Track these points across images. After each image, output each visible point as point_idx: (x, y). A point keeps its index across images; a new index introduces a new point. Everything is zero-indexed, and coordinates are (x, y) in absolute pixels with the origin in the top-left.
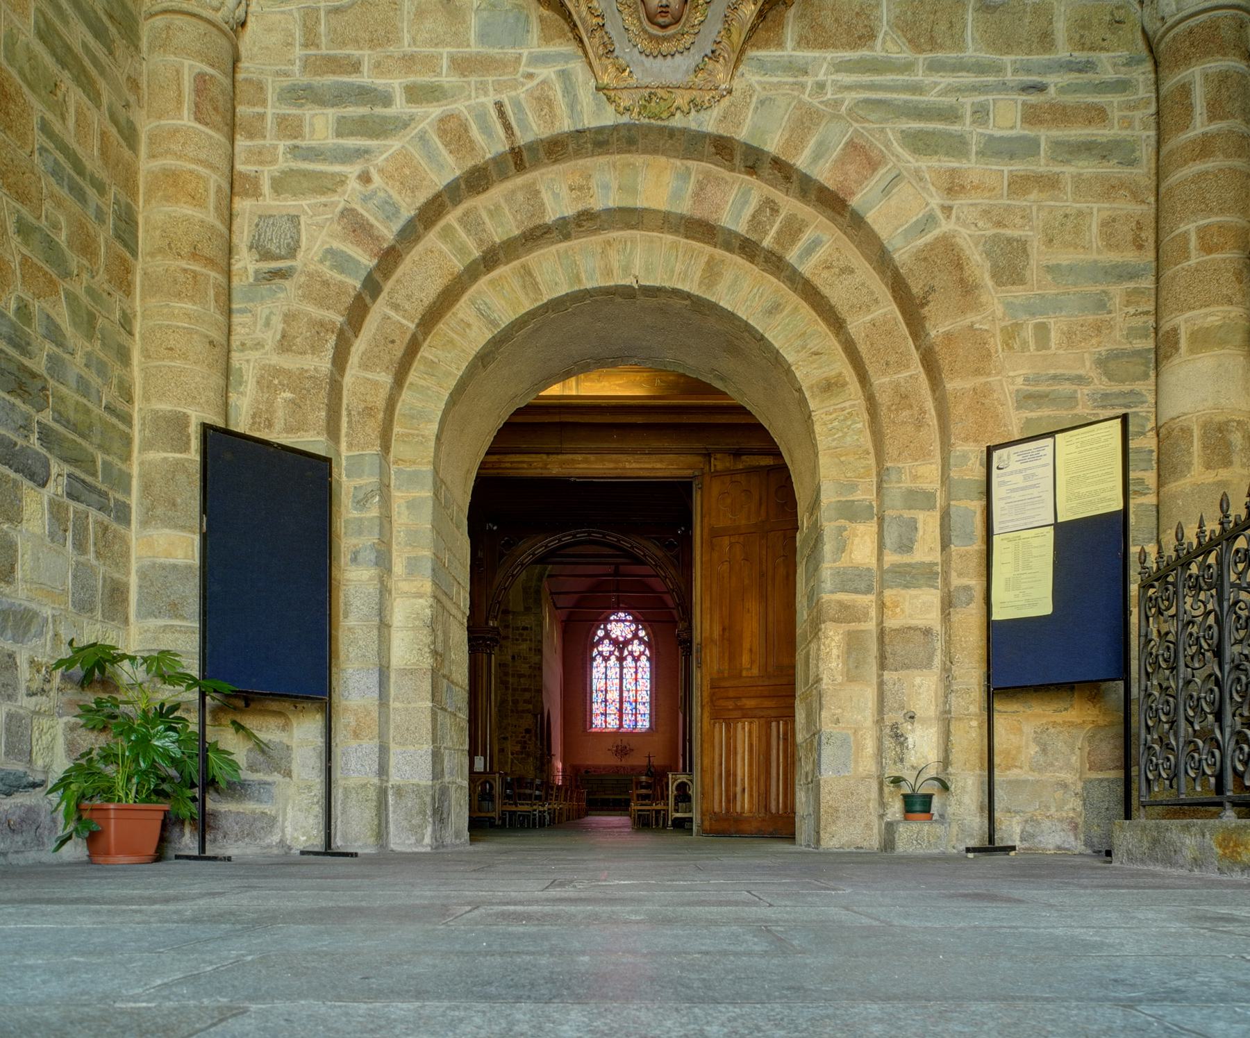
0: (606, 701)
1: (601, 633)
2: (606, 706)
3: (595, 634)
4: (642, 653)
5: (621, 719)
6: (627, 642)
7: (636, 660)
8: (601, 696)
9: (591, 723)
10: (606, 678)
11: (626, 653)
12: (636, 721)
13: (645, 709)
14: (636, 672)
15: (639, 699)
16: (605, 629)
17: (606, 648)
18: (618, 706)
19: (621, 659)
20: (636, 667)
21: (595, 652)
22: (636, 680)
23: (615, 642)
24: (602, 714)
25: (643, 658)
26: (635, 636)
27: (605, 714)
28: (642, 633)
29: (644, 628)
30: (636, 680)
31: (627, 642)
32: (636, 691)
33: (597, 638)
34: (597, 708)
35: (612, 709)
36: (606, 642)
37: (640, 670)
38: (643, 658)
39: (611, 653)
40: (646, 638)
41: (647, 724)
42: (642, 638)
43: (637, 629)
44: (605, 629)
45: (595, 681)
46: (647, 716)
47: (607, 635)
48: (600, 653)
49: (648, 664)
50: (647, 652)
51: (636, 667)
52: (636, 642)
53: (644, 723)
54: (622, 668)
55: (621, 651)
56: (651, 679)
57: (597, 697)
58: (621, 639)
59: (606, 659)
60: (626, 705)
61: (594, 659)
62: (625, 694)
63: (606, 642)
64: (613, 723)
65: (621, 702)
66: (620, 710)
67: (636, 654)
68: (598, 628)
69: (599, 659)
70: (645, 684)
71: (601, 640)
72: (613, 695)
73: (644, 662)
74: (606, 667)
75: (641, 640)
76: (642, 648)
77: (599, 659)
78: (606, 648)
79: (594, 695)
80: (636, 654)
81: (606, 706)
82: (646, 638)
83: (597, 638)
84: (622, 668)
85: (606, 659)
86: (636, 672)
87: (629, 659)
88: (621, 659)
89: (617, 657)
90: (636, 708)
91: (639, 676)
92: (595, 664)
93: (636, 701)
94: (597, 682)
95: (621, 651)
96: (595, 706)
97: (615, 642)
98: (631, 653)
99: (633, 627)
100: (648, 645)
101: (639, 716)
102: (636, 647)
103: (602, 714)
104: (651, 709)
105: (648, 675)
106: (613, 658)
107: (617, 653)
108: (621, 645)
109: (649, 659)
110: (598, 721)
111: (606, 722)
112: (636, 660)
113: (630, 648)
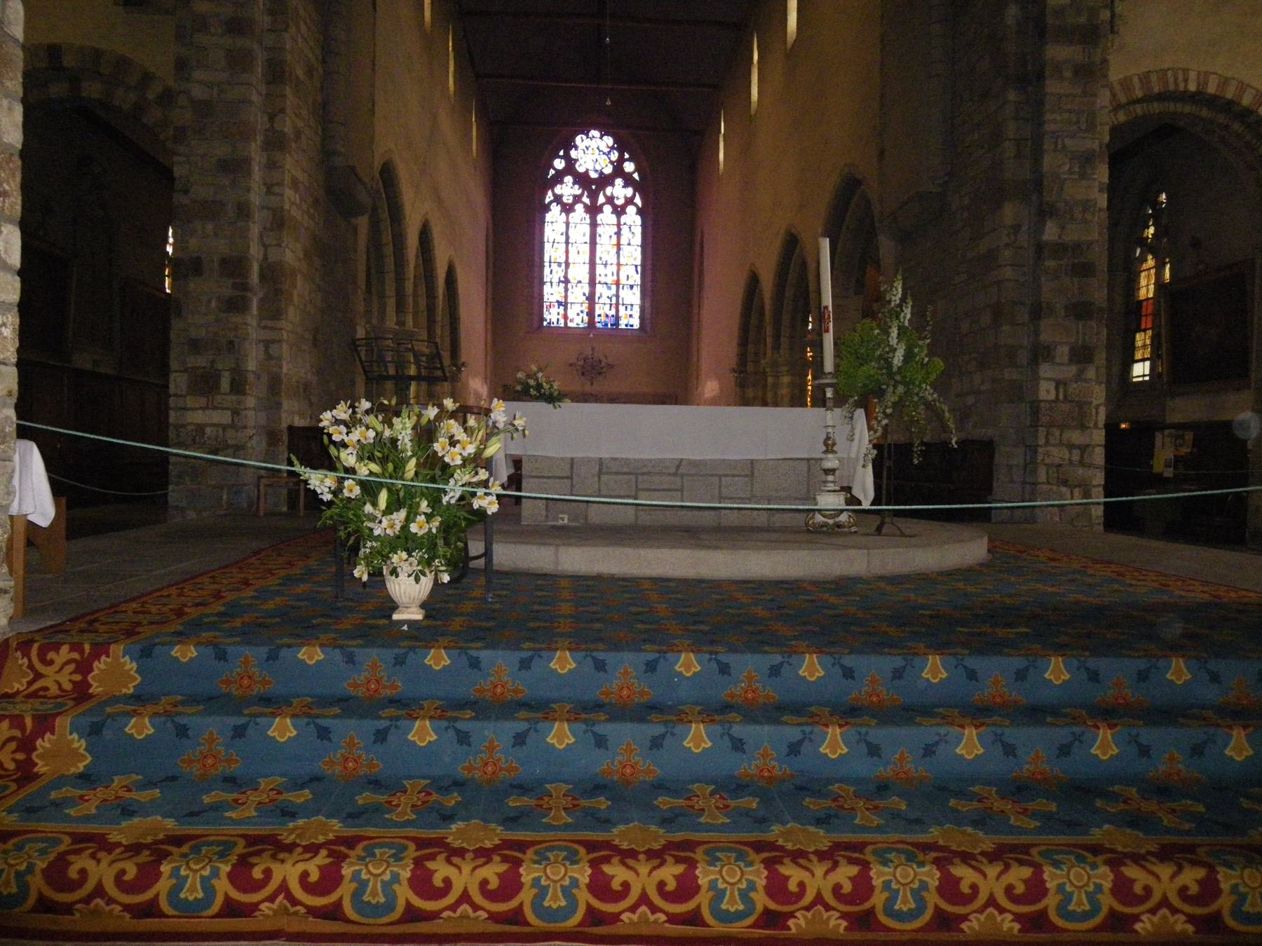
1: (559, 164)
2: (566, 290)
4: (629, 201)
5: (591, 313)
6: (605, 181)
7: (619, 211)
8: (559, 273)
9: (543, 319)
10: (567, 243)
11: (601, 199)
13: (633, 297)
14: (618, 234)
15: (623, 280)
16: (567, 157)
17: (568, 189)
18: (587, 290)
19: (594, 210)
20: (619, 225)
21: (549, 197)
22: (618, 245)
23: (582, 180)
25: (631, 210)
26: (618, 171)
27: (564, 304)
28: (629, 167)
30: (618, 245)
31: (605, 181)
32: (619, 265)
33: (552, 172)
34: (551, 293)
35: (578, 295)
36: (569, 179)
37: (625, 230)
39: (577, 199)
40: (636, 176)
41: (636, 323)
42: (630, 174)
43: (621, 160)
44: (567, 157)
45: (547, 247)
47: (571, 163)
48: (558, 199)
49: (638, 220)
50: (638, 200)
51: (619, 225)
53: (631, 319)
54: (594, 225)
55: (593, 196)
56: (644, 246)
57: (551, 274)
58: (594, 175)
59: (567, 209)
60: (599, 289)
61: (547, 208)
62: (600, 269)
63: (569, 179)
64: (577, 319)
65: (593, 283)
66: (591, 299)
67: (620, 202)
69: (555, 208)
70: (633, 254)
72: (579, 272)
73: (632, 217)
74: (567, 224)
75: (628, 181)
77: (555, 208)
78: (568, 189)
79: (547, 270)
81: (566, 290)
82: (636, 176)
83: (552, 172)
84: (594, 225)
85: (567, 209)
86: (618, 234)
87: (608, 209)
88: (594, 210)
89: (585, 206)
90: (617, 296)
91: (624, 241)
92: (549, 217)
93: (617, 283)
94: (552, 251)
95: (593, 196)
96: (547, 288)
97: (582, 180)
98: (610, 200)
99: (615, 156)
100: (638, 187)
101: (622, 308)
102: (620, 191)
103: (560, 303)
105: (638, 239)
106: (579, 208)
107: (586, 200)
108: (592, 185)
109: (640, 212)
110: (552, 316)
111: (565, 317)
112: (619, 211)
113: (609, 190)
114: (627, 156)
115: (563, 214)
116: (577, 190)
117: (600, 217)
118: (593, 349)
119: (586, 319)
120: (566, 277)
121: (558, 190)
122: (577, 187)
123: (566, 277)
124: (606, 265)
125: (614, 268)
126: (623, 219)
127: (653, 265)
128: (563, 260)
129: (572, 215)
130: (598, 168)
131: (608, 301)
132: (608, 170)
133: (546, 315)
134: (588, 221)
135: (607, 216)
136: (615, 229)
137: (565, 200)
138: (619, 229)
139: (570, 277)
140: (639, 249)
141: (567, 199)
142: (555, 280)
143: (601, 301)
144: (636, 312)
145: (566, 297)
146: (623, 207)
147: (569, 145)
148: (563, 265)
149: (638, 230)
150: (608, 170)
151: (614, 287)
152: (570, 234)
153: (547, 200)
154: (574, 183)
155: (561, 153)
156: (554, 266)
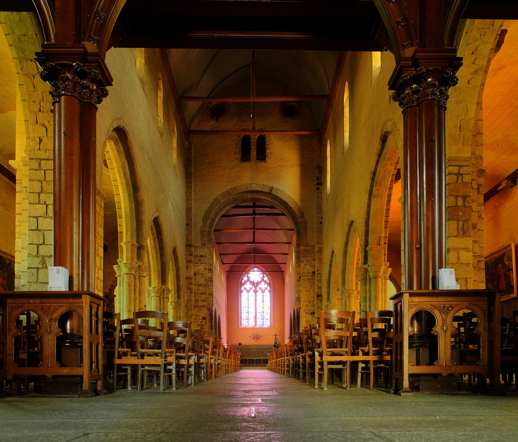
0: (248, 312)
1: (245, 279)
2: (248, 315)
3: (242, 279)
4: (266, 289)
6: (258, 283)
7: (263, 292)
11: (258, 288)
12: (263, 322)
13: (268, 316)
16: (248, 276)
18: (254, 315)
19: (256, 292)
20: (263, 296)
21: (243, 288)
23: (253, 283)
24: (246, 319)
25: (267, 291)
26: (263, 280)
28: (266, 279)
29: (267, 276)
31: (258, 283)
34: (244, 316)
36: (248, 283)
38: (267, 291)
39: (251, 289)
41: (269, 324)
42: (266, 281)
43: (263, 277)
44: (248, 276)
46: (269, 320)
47: (248, 280)
48: (245, 289)
49: (269, 294)
50: (269, 288)
51: (263, 296)
52: (263, 283)
53: (267, 324)
54: (256, 296)
55: (256, 287)
58: (256, 282)
59: (248, 292)
60: (258, 314)
61: (242, 292)
62: (258, 309)
63: (248, 283)
64: (252, 324)
67: (263, 289)
68: (244, 276)
69: (245, 291)
71: (245, 282)
72: (252, 310)
73: (267, 294)
75: (265, 282)
76: (266, 286)
77: (245, 291)
78: (248, 286)
80: (263, 289)
81: (248, 315)
82: (268, 281)
83: (243, 281)
84: (256, 296)
85: (248, 292)
87: (260, 291)
88: (256, 292)
90: (263, 316)
92: (243, 294)
95: (256, 287)
96: (242, 315)
97: (253, 283)
98: (260, 289)
100: (269, 284)
101: (264, 319)
102: (263, 286)
103: (246, 319)
104: (271, 316)
106: (252, 291)
107: (254, 289)
108: (255, 285)
109: (270, 291)
110: (244, 323)
111: (248, 322)
112: (263, 292)
113: (260, 286)
114: (265, 275)
115: (247, 293)
116: (251, 286)
117: (257, 294)
118: (256, 332)
119: (254, 323)
120: (248, 311)
121: (245, 286)
122: (251, 285)
123: (248, 311)
124: (259, 307)
125: (262, 308)
126: (264, 294)
127: (273, 319)
128: (247, 306)
129: (249, 293)
130: (257, 279)
131: (260, 318)
132: (260, 280)
133: (242, 322)
134: (254, 295)
135: (259, 293)
136: (262, 297)
137: (247, 289)
138: (263, 297)
139: (249, 311)
140: (269, 302)
141: (248, 289)
142: (245, 312)
143: (258, 318)
144: (269, 321)
145: (248, 317)
146: (264, 290)
147: (248, 274)
148: (247, 308)
149: (269, 297)
150: (260, 280)
151: (262, 314)
152: (249, 299)
153: (242, 290)
154: (250, 284)
155: (246, 275)
156: (245, 308)
